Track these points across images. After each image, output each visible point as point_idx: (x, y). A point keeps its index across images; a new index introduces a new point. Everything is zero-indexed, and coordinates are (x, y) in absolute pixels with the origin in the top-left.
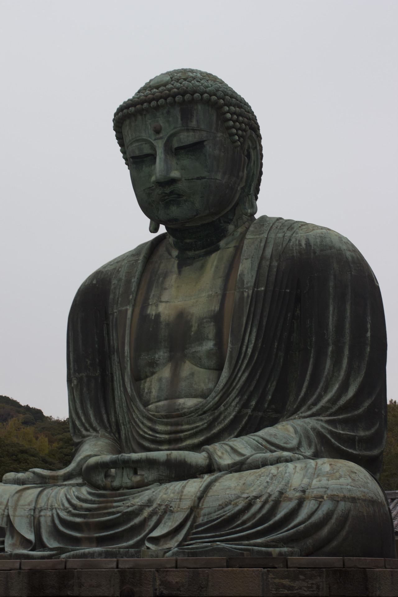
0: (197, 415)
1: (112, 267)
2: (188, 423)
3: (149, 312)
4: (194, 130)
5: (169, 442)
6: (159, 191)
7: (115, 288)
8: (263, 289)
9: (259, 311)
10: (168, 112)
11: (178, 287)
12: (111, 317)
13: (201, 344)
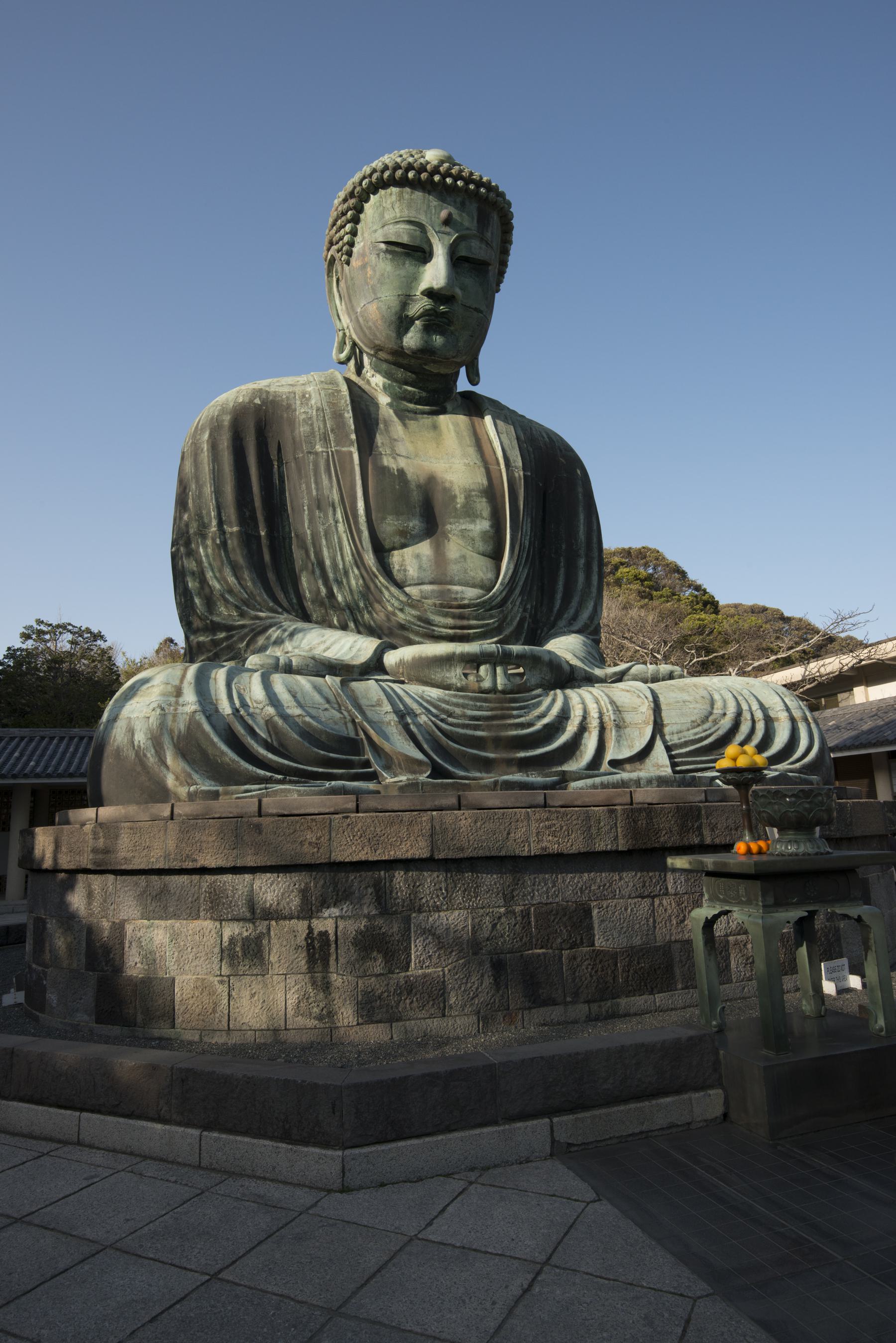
1: (286, 390)
4: (487, 244)
10: (463, 204)
11: (412, 442)
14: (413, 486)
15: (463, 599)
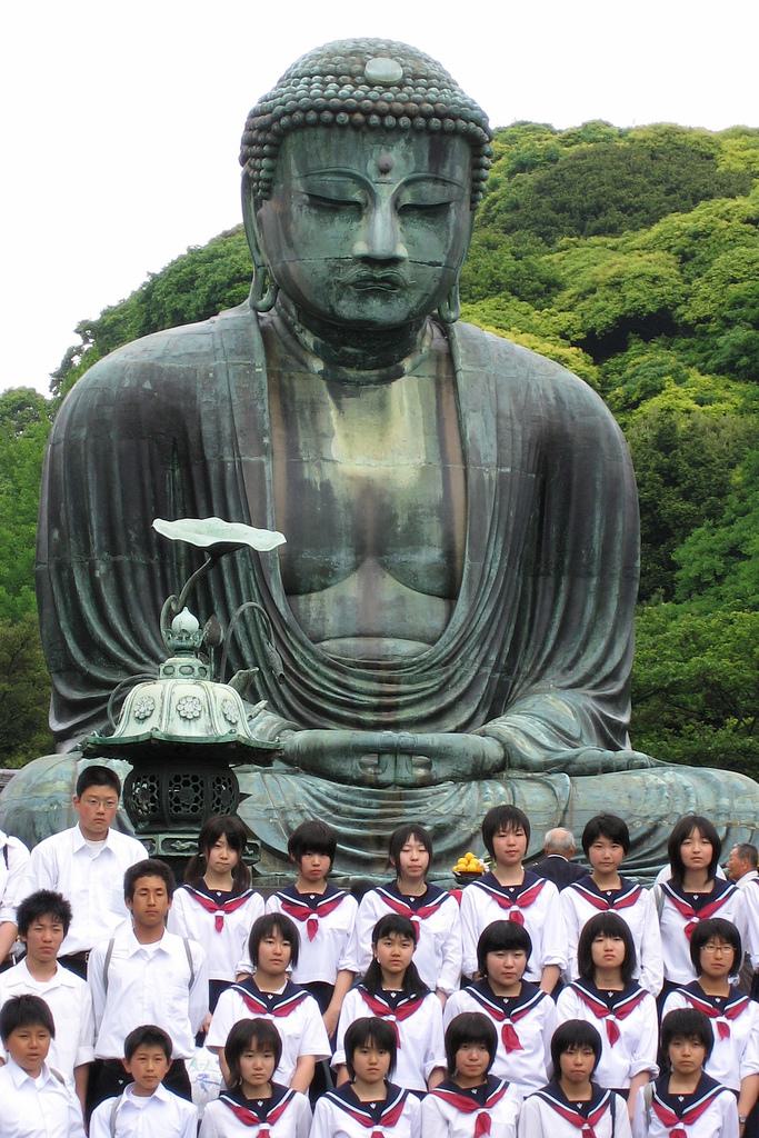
0: (420, 670)
2: (409, 683)
3: (306, 475)
4: (444, 182)
6: (364, 272)
7: (215, 411)
8: (508, 470)
9: (505, 509)
10: (408, 142)
11: (346, 436)
12: (213, 468)
14: (340, 506)
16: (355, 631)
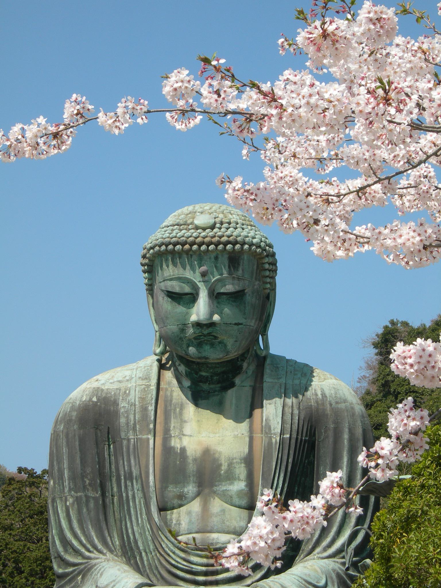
1: (115, 386)
3: (173, 444)
5: (206, 574)
7: (126, 412)
8: (288, 436)
10: (216, 258)
11: (198, 421)
12: (125, 442)
13: (232, 484)
14: (190, 460)
15: (217, 543)
16: (195, 529)
